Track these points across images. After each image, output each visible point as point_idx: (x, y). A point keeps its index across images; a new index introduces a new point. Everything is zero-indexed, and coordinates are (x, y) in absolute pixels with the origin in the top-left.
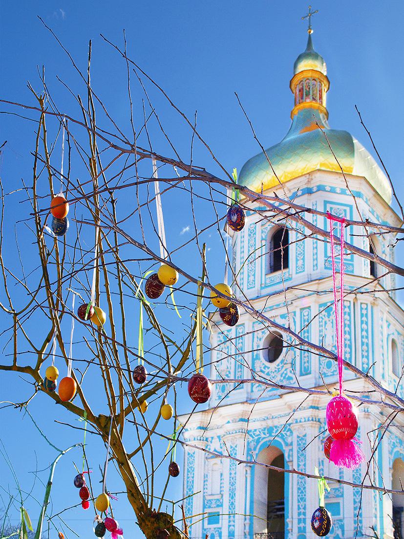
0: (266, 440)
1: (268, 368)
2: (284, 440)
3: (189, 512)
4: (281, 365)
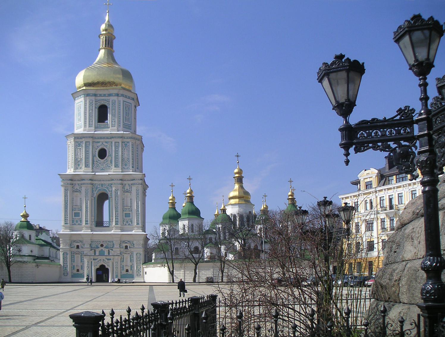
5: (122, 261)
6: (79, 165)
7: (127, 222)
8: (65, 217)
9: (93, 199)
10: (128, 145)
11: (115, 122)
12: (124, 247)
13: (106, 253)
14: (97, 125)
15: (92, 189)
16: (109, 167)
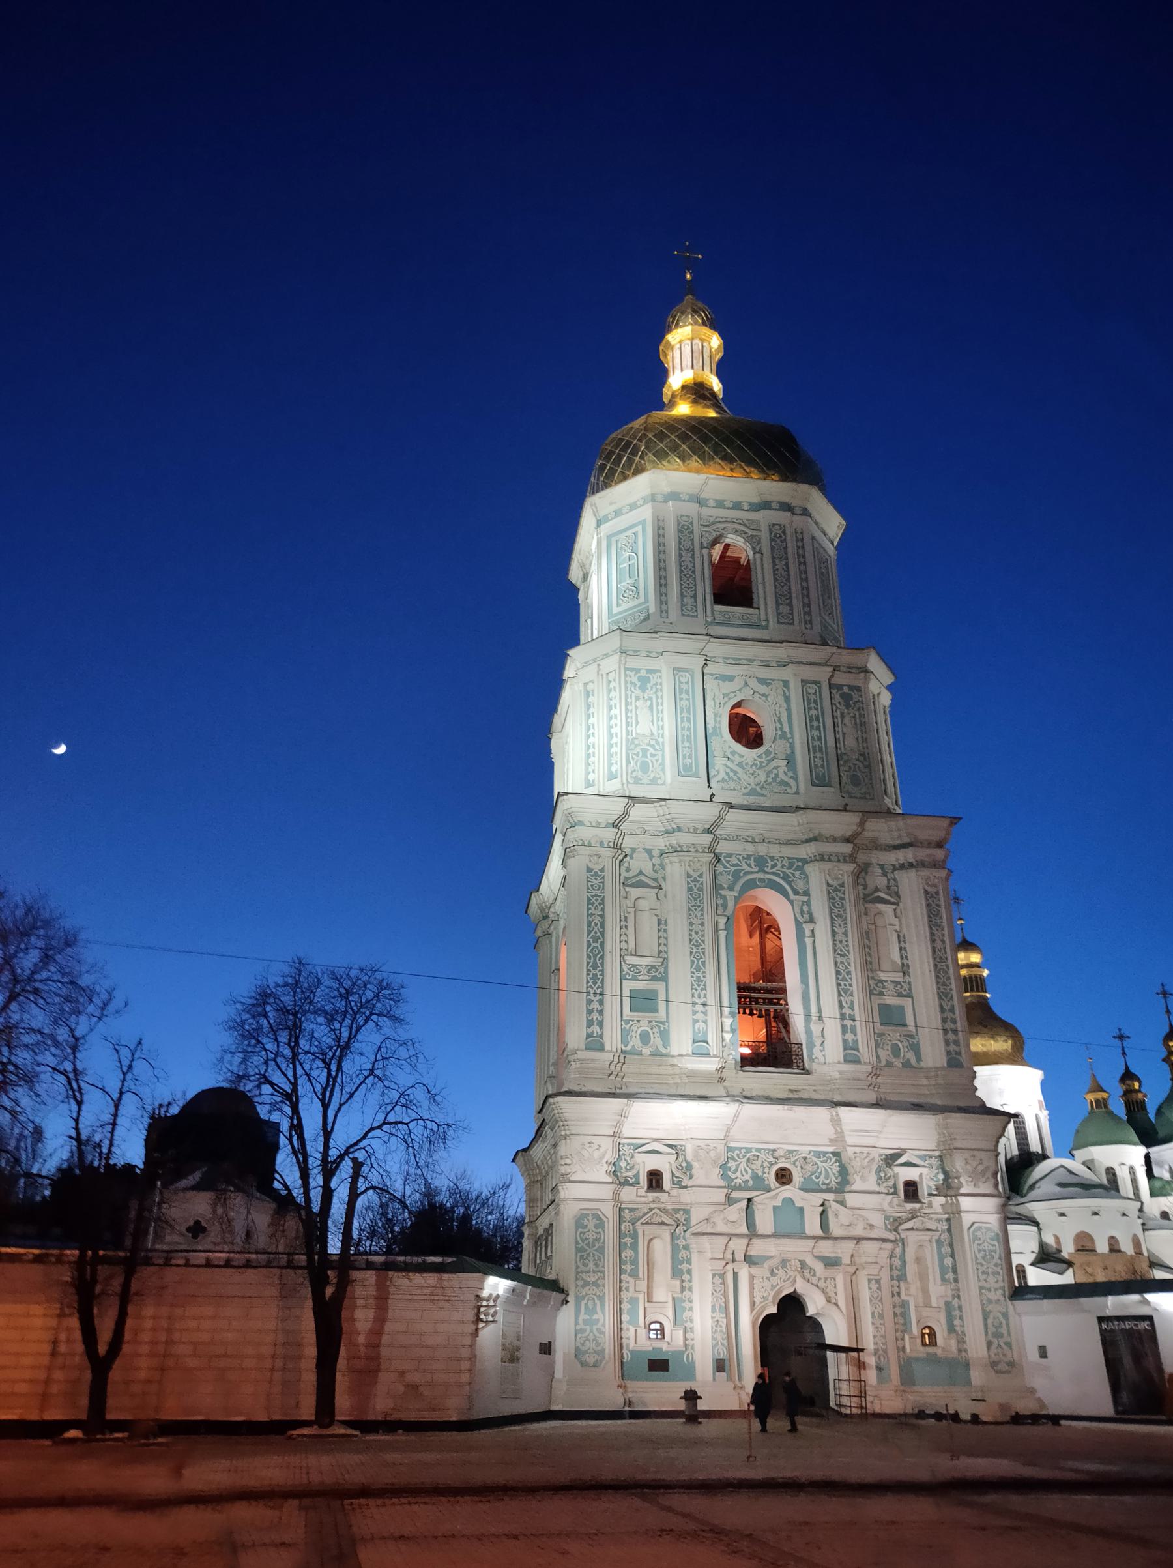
0: (750, 877)
1: (741, 756)
2: (789, 883)
3: (595, 983)
5: (896, 1273)
8: (590, 1012)
10: (855, 696)
11: (790, 605)
13: (813, 1225)
16: (782, 783)
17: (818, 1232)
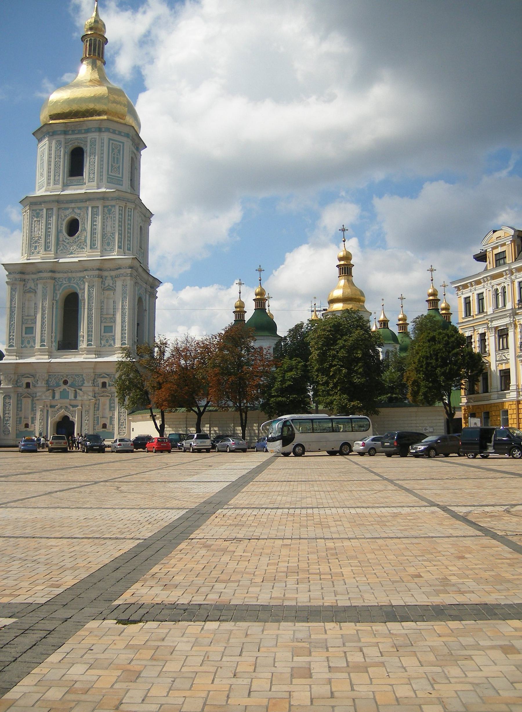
2: (79, 287)
4: (77, 239)
6: (36, 248)
7: (107, 341)
8: (10, 336)
9: (55, 304)
10: (113, 210)
11: (94, 173)
12: (100, 385)
13: (71, 396)
14: (67, 180)
15: (54, 286)
17: (73, 398)
